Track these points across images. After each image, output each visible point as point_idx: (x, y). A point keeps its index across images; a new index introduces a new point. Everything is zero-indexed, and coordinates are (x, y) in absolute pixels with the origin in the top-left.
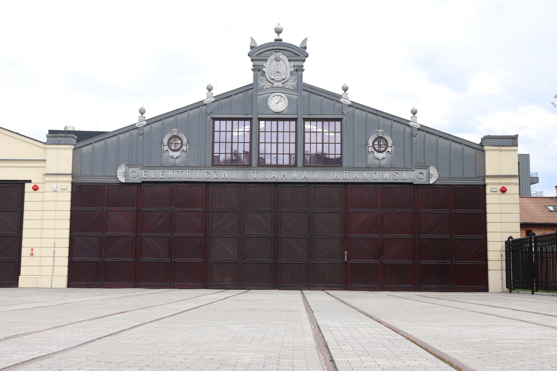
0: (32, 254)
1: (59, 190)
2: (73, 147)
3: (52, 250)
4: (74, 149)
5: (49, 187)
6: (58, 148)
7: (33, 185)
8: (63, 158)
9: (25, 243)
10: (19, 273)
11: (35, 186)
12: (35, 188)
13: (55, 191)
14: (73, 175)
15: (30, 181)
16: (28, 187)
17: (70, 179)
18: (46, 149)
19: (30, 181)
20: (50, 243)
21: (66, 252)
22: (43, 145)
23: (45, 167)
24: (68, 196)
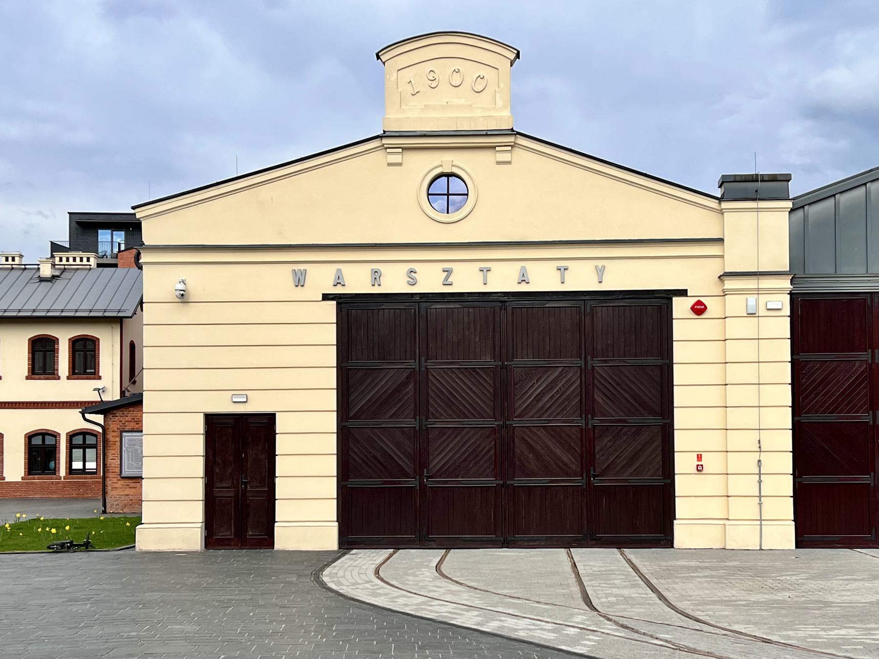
0: (700, 469)
1: (762, 312)
2: (789, 204)
3: (756, 456)
4: (792, 211)
5: (735, 304)
6: (758, 210)
7: (693, 301)
8: (764, 236)
9: (680, 441)
10: (673, 516)
11: (699, 303)
12: (699, 309)
13: (751, 315)
14: (795, 274)
15: (683, 293)
16: (680, 307)
17: (785, 284)
18: (721, 212)
19: (683, 293)
20: (748, 440)
21: (787, 462)
22: (713, 204)
23: (722, 257)
24: (783, 327)
